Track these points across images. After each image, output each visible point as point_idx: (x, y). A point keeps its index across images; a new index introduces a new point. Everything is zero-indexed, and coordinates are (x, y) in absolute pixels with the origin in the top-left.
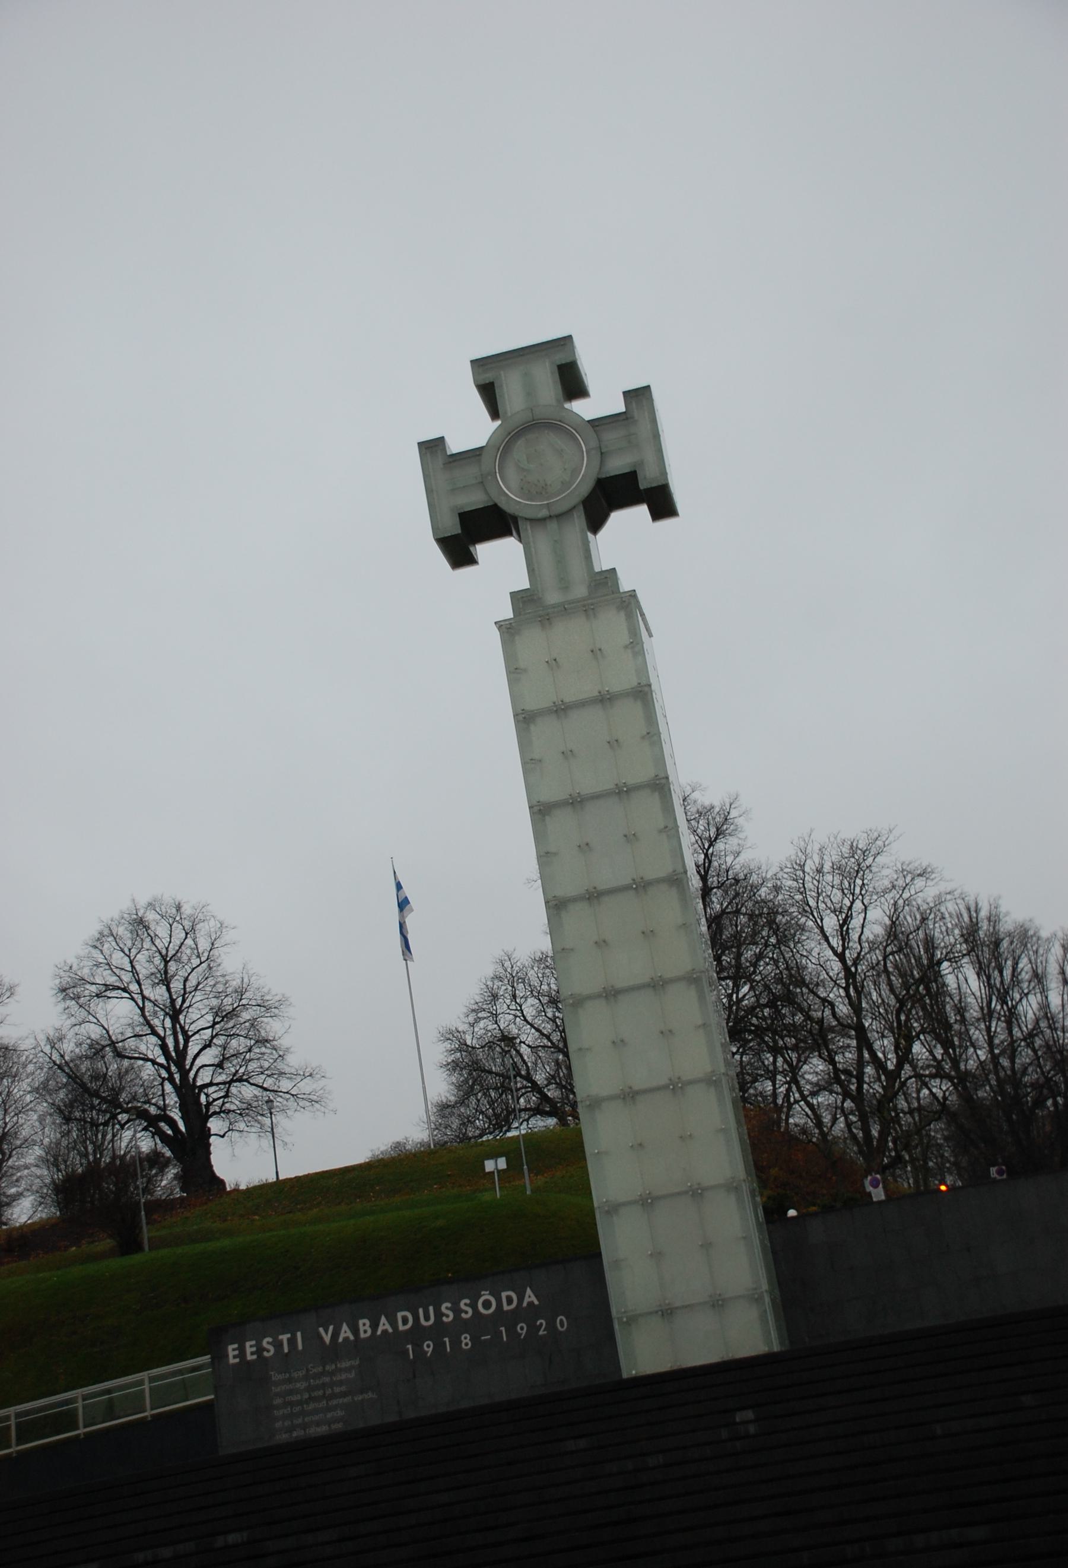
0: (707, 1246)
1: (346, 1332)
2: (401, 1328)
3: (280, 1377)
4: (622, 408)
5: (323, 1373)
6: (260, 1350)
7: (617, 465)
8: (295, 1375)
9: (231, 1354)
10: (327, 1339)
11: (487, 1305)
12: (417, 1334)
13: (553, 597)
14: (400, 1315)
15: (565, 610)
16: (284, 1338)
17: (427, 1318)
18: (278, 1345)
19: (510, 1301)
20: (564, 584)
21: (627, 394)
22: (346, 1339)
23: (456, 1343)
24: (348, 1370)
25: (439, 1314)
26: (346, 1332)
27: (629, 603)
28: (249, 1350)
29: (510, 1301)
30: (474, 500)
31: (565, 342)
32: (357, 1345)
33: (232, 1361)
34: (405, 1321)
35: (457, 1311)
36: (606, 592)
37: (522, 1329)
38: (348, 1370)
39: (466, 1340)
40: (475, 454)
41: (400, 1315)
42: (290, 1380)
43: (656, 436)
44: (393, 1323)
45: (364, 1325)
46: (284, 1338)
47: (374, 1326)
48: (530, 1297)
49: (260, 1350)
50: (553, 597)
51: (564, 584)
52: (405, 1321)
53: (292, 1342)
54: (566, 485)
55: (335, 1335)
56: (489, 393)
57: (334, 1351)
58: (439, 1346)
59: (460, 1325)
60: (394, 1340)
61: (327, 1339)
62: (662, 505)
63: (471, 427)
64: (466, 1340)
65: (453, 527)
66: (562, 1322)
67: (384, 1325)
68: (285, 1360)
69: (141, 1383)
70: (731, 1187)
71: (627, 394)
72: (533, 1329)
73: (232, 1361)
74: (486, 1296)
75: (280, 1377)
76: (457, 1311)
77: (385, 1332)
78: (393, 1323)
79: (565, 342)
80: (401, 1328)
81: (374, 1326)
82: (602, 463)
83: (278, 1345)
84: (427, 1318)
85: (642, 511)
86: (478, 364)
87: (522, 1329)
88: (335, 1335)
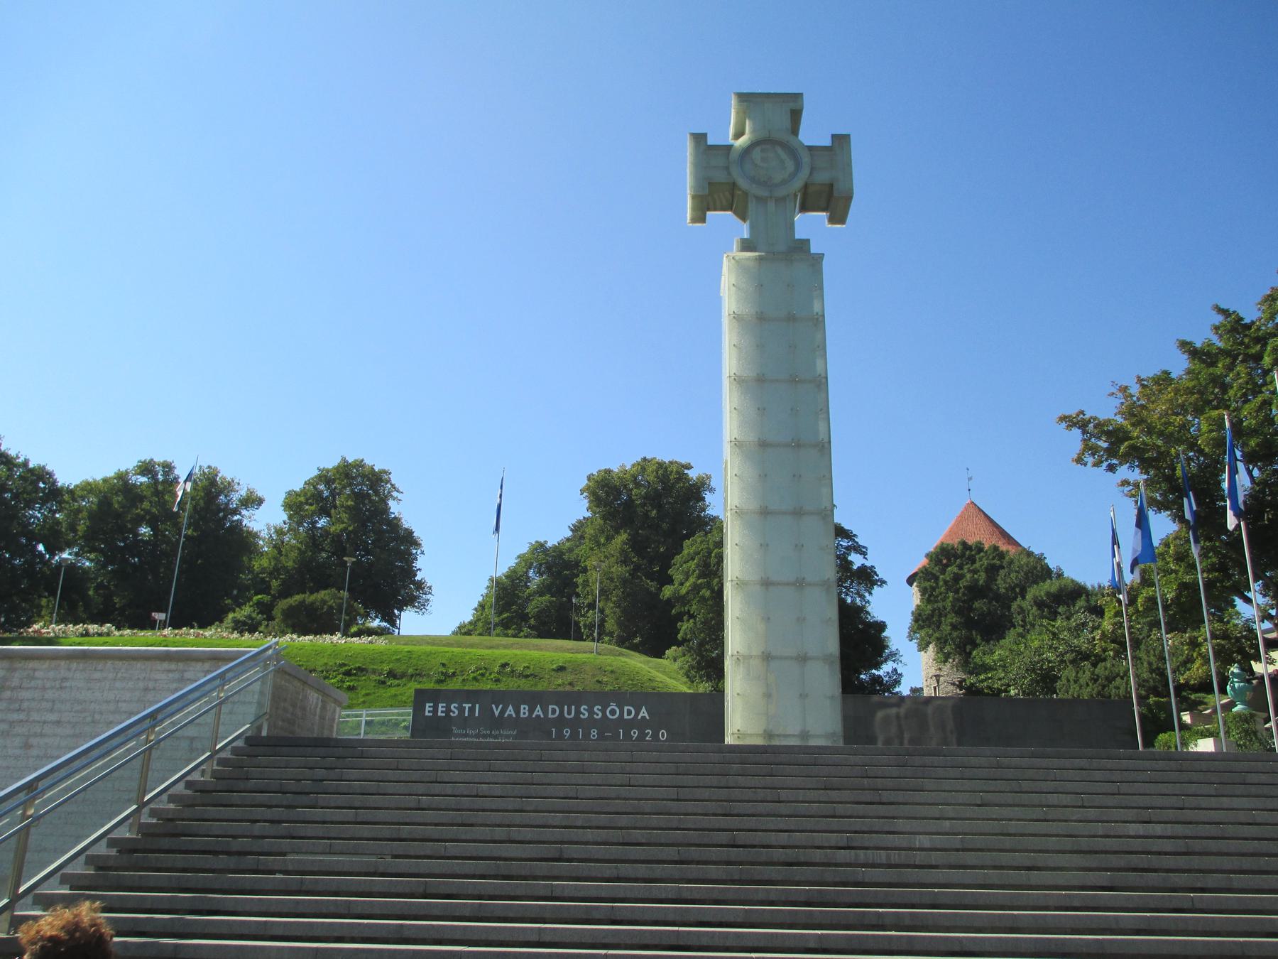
0: (803, 696)
1: (510, 711)
2: (550, 716)
3: (461, 731)
4: (827, 142)
5: (490, 735)
6: (448, 711)
7: (822, 177)
8: (469, 732)
9: (427, 709)
10: (497, 713)
11: (613, 712)
12: (561, 722)
14: (550, 707)
16: (467, 706)
17: (569, 713)
18: (461, 710)
19: (629, 713)
21: (833, 136)
22: (510, 716)
23: (587, 735)
24: (507, 736)
25: (578, 712)
26: (510, 711)
28: (440, 709)
29: (629, 713)
30: (720, 177)
31: (797, 97)
33: (427, 714)
34: (554, 711)
35: (591, 712)
37: (635, 734)
38: (507, 736)
39: (594, 733)
41: (550, 707)
42: (466, 735)
43: (850, 165)
44: (545, 711)
45: (524, 709)
46: (467, 706)
47: (531, 711)
48: (644, 713)
49: (448, 711)
52: (554, 711)
53: (472, 710)
54: (784, 182)
55: (503, 711)
57: (500, 722)
58: (574, 735)
59: (591, 722)
61: (497, 713)
64: (594, 733)
66: (663, 735)
67: (538, 711)
68: (464, 721)
69: (360, 716)
70: (826, 659)
71: (833, 136)
72: (642, 736)
73: (427, 714)
74: (613, 706)
75: (461, 731)
76: (591, 712)
77: (538, 716)
78: (545, 711)
79: (797, 97)
80: (550, 716)
81: (531, 711)
82: (811, 174)
83: (461, 710)
84: (569, 713)
87: (635, 734)
88: (503, 711)
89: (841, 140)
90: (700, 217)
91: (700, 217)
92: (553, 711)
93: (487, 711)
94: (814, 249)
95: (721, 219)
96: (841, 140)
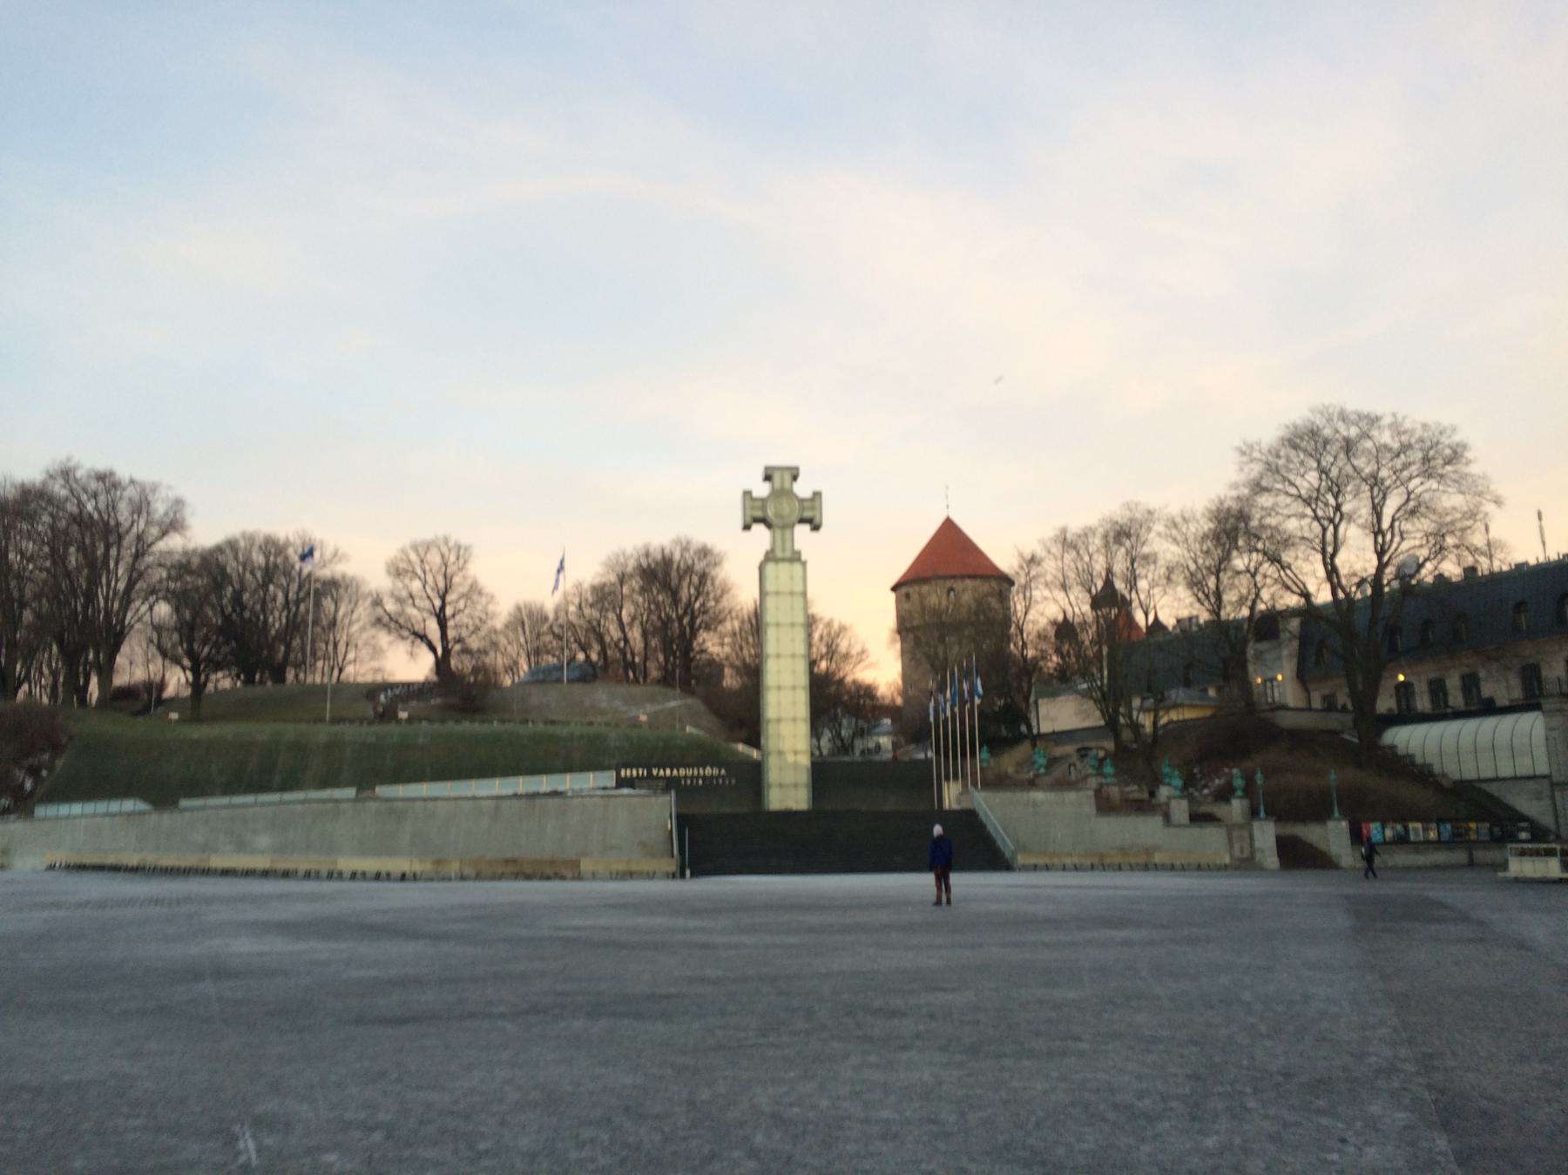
7: (807, 514)
12: (686, 777)
13: (779, 554)
15: (783, 560)
20: (784, 550)
27: (804, 564)
30: (759, 514)
31: (797, 469)
32: (665, 778)
36: (796, 558)
40: (763, 500)
45: (668, 772)
50: (779, 554)
51: (784, 550)
56: (768, 478)
57: (658, 777)
59: (698, 777)
60: (678, 779)
62: (816, 528)
63: (762, 490)
65: (749, 520)
79: (797, 469)
85: (807, 527)
86: (767, 469)
89: (817, 495)
90: (747, 527)
91: (747, 527)
92: (682, 772)
93: (650, 772)
94: (804, 557)
95: (759, 529)
96: (817, 495)
